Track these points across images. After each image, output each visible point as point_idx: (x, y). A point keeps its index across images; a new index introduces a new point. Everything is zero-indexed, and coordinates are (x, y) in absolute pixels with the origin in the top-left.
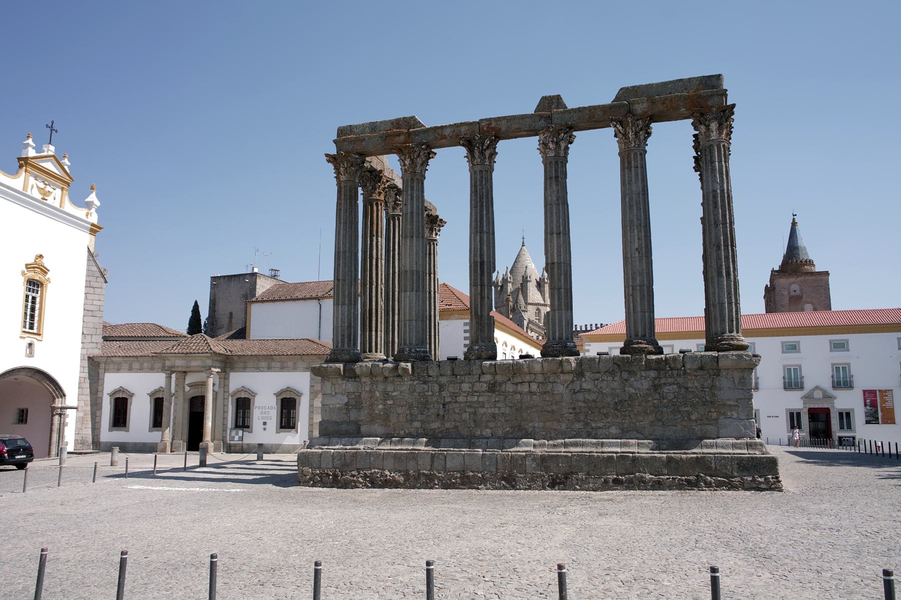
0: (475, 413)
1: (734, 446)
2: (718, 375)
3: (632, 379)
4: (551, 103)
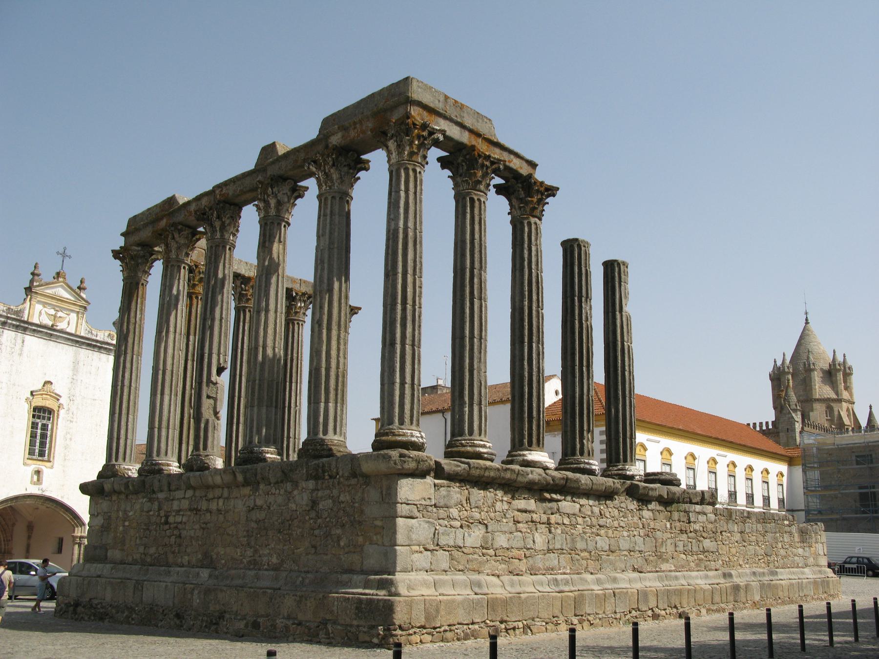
0: (180, 536)
3: (295, 492)
4: (269, 150)
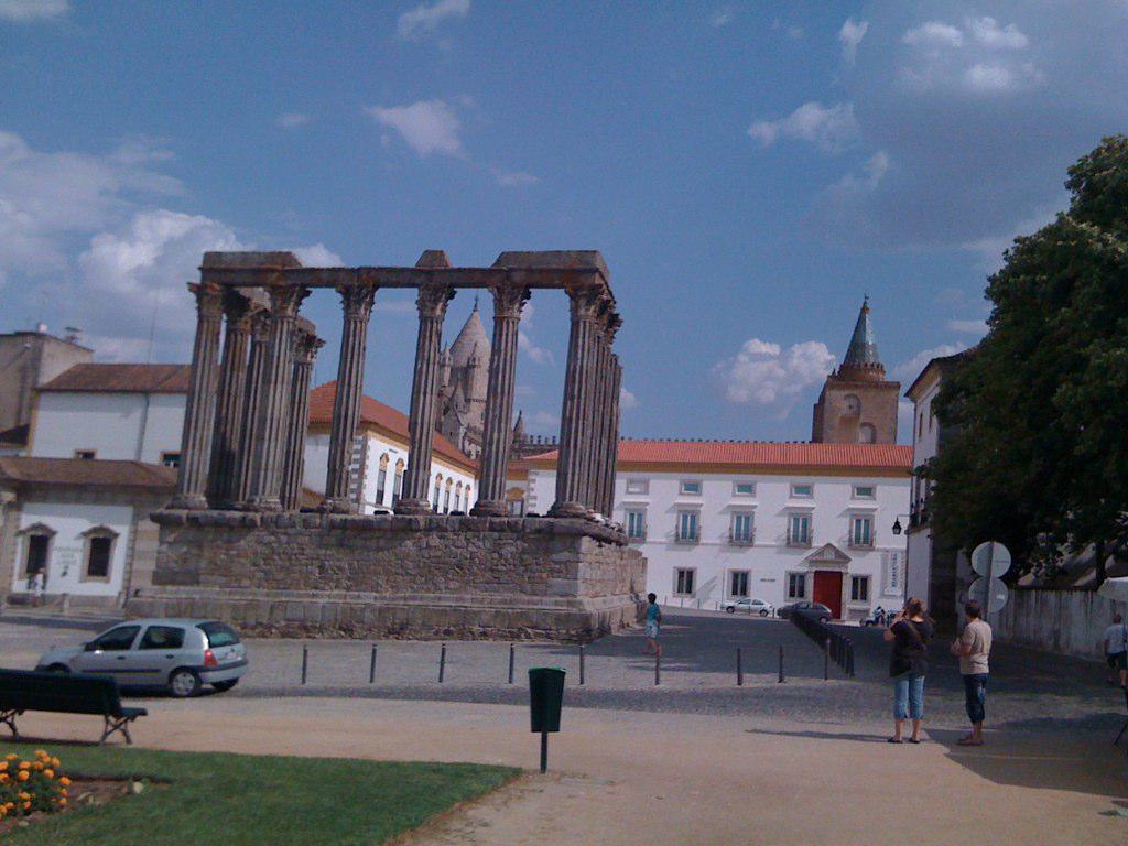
1: (556, 603)
2: (552, 539)
